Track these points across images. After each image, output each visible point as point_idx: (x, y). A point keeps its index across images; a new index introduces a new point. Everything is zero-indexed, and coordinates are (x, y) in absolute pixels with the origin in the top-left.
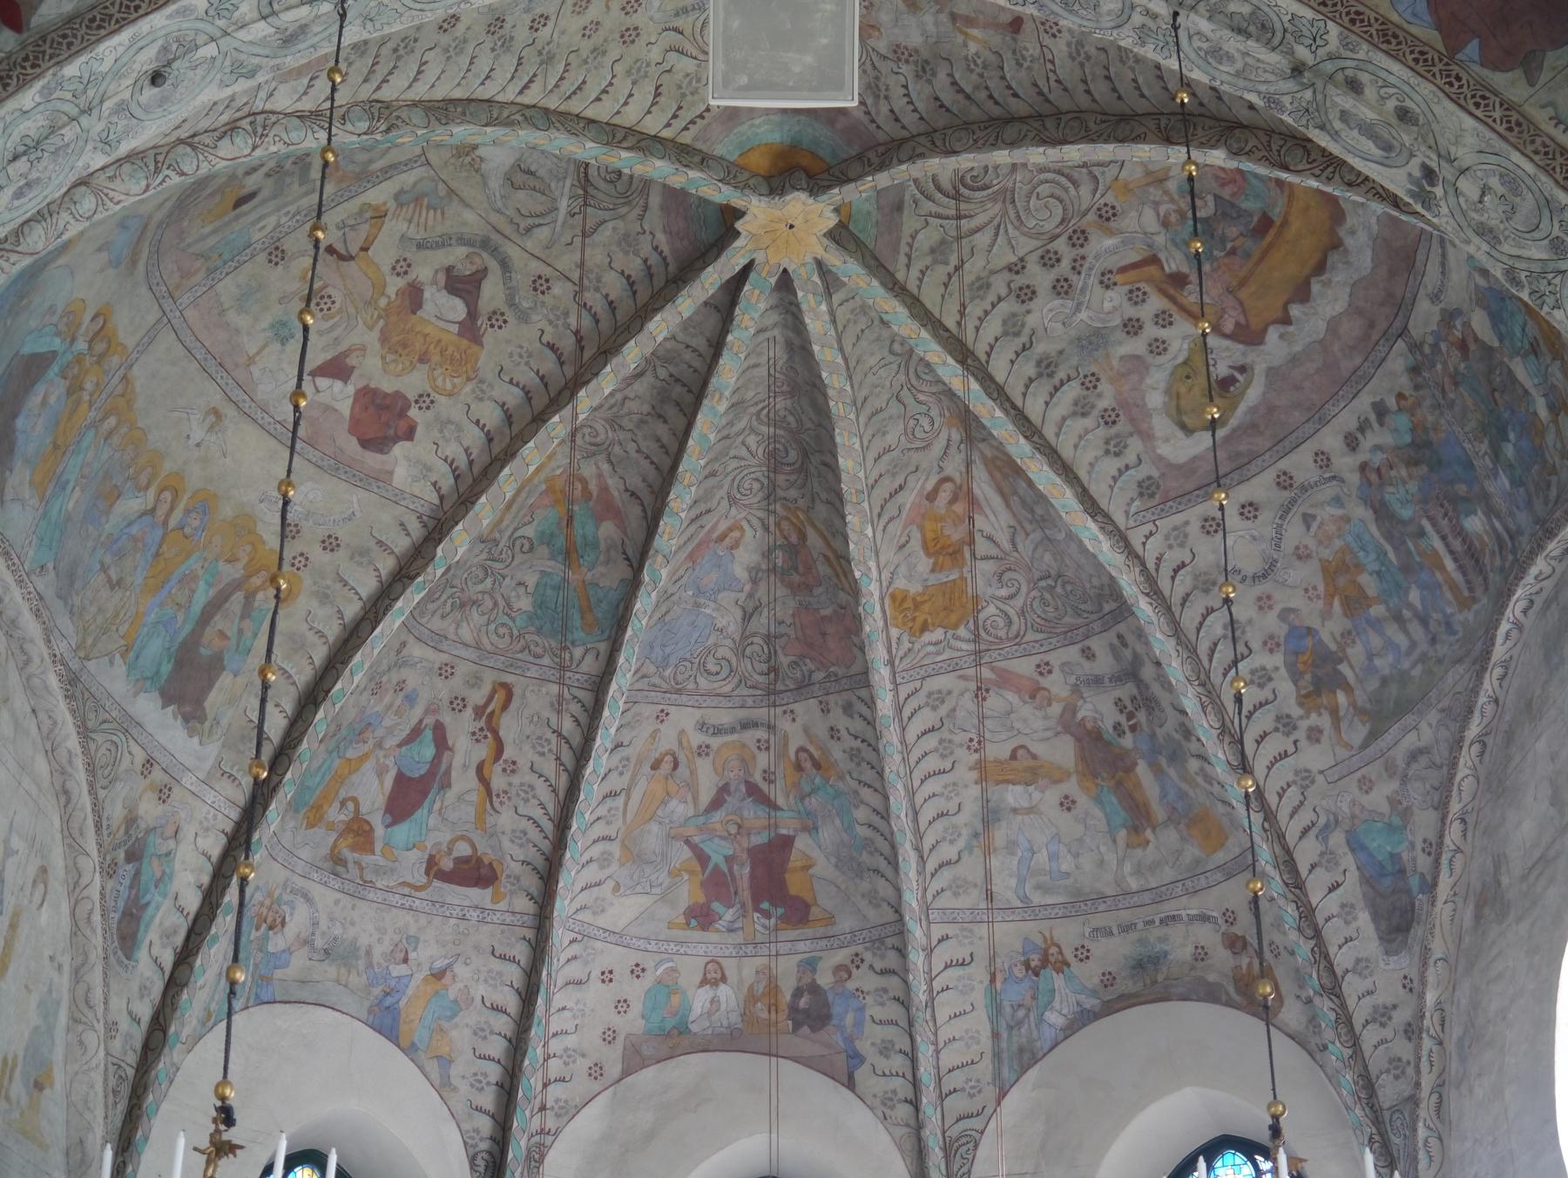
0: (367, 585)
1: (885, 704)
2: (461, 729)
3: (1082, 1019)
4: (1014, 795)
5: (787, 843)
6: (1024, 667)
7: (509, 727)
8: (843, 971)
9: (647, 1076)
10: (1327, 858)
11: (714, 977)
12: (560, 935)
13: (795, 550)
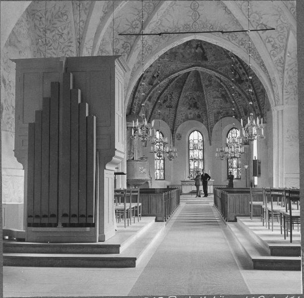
0: (162, 89)
1: (205, 94)
2: (169, 96)
3: (221, 118)
4: (216, 99)
5: (196, 103)
6: (217, 89)
7: (173, 95)
8: (202, 113)
9: (185, 122)
10: (241, 108)
11: (190, 114)
12: (178, 112)
13: (197, 81)
